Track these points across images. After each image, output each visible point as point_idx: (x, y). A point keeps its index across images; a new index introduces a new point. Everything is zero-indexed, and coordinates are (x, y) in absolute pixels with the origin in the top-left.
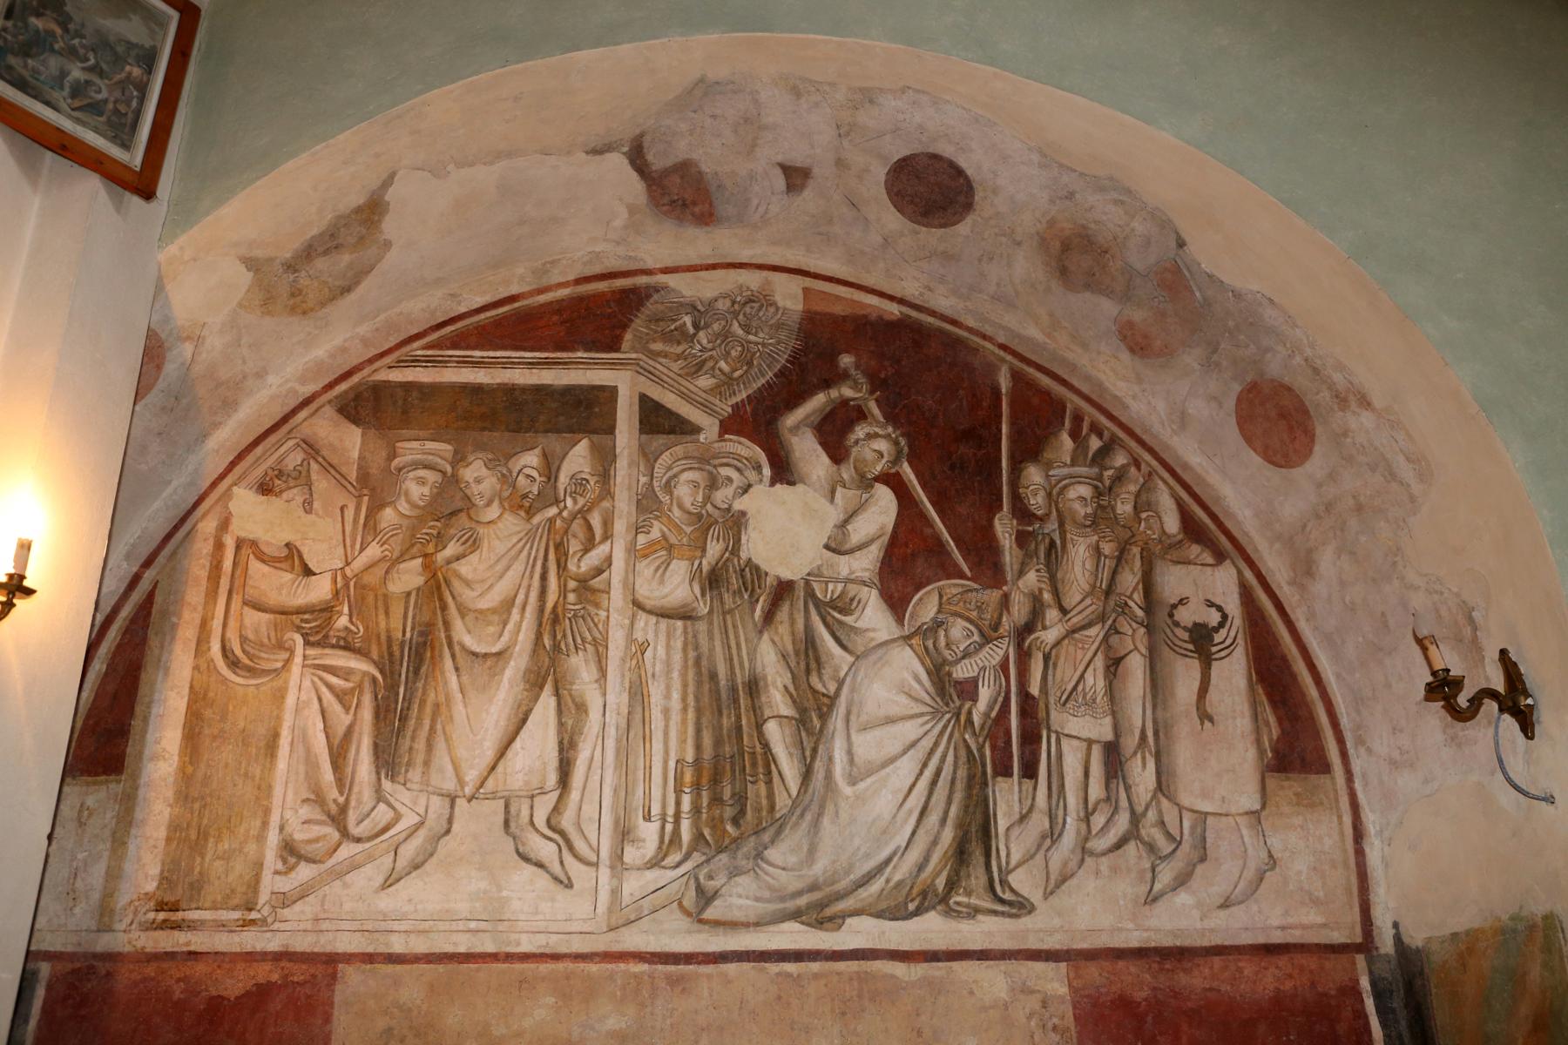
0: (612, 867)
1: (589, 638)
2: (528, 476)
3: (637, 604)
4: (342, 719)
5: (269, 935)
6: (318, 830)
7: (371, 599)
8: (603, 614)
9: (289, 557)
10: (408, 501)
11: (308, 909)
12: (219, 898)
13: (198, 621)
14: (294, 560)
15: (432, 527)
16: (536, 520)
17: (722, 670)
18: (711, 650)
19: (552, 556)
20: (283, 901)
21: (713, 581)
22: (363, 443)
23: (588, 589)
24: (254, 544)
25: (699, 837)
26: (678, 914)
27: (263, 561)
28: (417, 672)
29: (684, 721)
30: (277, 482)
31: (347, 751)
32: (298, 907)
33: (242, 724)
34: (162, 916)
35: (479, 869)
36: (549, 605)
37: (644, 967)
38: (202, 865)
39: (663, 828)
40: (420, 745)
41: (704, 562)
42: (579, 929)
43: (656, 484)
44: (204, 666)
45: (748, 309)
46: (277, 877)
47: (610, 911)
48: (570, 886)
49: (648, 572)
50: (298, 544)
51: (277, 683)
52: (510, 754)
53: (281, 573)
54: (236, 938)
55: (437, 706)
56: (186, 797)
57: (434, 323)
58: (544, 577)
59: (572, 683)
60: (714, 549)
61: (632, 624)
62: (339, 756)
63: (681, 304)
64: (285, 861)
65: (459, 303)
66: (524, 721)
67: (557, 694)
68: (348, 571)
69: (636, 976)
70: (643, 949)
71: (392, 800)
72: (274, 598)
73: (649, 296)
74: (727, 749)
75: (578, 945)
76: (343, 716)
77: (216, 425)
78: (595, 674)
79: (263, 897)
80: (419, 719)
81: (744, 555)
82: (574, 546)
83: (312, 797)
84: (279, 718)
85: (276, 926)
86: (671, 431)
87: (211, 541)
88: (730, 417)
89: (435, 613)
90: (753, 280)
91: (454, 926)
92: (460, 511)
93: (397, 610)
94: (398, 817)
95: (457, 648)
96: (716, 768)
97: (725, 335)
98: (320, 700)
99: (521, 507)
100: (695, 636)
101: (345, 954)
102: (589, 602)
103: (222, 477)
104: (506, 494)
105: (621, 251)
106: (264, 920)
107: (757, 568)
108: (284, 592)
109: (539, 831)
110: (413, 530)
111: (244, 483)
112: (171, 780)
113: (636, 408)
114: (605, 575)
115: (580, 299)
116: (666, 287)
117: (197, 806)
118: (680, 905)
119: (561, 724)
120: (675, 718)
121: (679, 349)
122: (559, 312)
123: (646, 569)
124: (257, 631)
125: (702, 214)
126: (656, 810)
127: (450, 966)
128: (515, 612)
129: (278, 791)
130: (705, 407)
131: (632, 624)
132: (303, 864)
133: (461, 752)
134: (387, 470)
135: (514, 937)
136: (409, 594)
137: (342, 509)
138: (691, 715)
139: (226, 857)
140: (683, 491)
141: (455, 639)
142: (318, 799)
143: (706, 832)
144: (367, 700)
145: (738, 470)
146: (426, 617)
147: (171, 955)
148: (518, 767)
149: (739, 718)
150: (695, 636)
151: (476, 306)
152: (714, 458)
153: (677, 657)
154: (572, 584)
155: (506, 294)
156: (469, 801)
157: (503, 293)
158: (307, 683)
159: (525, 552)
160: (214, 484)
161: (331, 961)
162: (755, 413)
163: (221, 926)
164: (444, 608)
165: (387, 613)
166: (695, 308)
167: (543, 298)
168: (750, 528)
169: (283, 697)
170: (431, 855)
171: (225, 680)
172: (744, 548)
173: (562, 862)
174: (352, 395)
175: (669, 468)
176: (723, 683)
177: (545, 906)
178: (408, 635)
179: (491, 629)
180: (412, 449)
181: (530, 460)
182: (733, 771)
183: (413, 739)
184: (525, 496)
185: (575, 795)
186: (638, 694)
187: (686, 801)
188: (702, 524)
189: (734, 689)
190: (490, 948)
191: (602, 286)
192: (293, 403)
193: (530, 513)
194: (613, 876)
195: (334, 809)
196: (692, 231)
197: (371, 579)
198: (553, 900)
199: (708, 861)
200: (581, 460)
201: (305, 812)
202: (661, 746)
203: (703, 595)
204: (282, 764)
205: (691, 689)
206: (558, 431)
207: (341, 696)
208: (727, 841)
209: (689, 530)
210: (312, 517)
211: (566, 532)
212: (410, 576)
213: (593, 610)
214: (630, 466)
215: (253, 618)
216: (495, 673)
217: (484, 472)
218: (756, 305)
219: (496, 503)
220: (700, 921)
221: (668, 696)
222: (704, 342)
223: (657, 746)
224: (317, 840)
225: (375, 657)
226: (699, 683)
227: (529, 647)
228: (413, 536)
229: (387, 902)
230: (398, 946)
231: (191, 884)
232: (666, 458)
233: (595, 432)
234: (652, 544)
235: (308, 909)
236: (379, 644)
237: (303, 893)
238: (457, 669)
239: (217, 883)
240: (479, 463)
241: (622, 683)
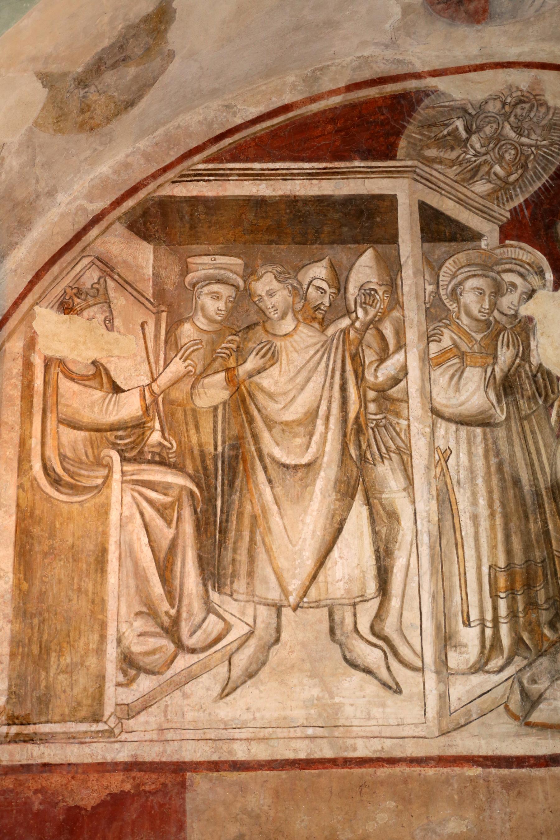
0: (438, 672)
1: (393, 447)
2: (318, 288)
3: (436, 413)
4: (165, 533)
5: (117, 745)
6: (152, 643)
7: (180, 414)
8: (404, 423)
9: (97, 375)
10: (205, 316)
11: (152, 719)
12: (67, 711)
13: (17, 440)
14: (101, 377)
15: (229, 342)
16: (330, 331)
17: (524, 476)
18: (512, 456)
19: (349, 367)
20: (129, 712)
21: (507, 387)
22: (155, 260)
23: (388, 398)
24: (61, 362)
25: (518, 641)
26: (506, 718)
27: (72, 380)
28: (232, 484)
29: (493, 527)
30: (77, 301)
31: (173, 564)
32: (142, 718)
33: (70, 541)
34: (14, 730)
35: (310, 677)
36: (352, 415)
37: (479, 771)
38: (47, 678)
39: (483, 632)
40: (243, 556)
41: (497, 369)
42: (411, 734)
43: (442, 292)
44: (27, 485)
45: (518, 111)
46: (120, 689)
47: (440, 715)
48: (398, 691)
49: (443, 380)
50: (104, 362)
51: (100, 499)
52: (329, 563)
53: (90, 390)
54: (86, 749)
55: (254, 518)
56: (25, 613)
57: (212, 136)
58: (343, 388)
59: (381, 492)
60: (505, 356)
61: (433, 432)
62: (166, 568)
63: (452, 108)
64: (125, 673)
65: (235, 114)
66: (340, 530)
67: (368, 503)
68: (155, 386)
69: (471, 780)
70: (476, 753)
71: (221, 611)
72: (88, 416)
73: (420, 101)
74: (537, 553)
75: (412, 750)
76: (166, 530)
77: (13, 245)
78: (402, 483)
79: (109, 709)
80: (239, 531)
81: (534, 361)
82: (370, 357)
83: (145, 610)
84: (105, 534)
85: (124, 736)
86: (452, 239)
87: (20, 361)
88: (509, 222)
89: (242, 426)
90: (522, 79)
91: (292, 733)
92: (257, 324)
93: (207, 425)
94: (228, 628)
95: (268, 460)
96: (528, 573)
97: (498, 139)
98: (142, 514)
99: (314, 319)
100: (495, 443)
101: (191, 763)
102: (389, 411)
103: (23, 296)
104: (299, 306)
105: (389, 54)
106: (111, 732)
107: (549, 373)
108: (96, 409)
109: (363, 637)
110: (213, 344)
111: (45, 303)
112: (9, 596)
113: (417, 216)
114: (403, 384)
115: (353, 106)
116: (435, 91)
117: (36, 621)
118: (507, 708)
119: (375, 533)
120: (484, 524)
121: (453, 155)
122: (332, 120)
123: (441, 377)
124: (74, 449)
125: (476, 12)
126: (474, 615)
127: (293, 772)
128: (320, 422)
129: (112, 605)
130: (483, 212)
131: (433, 432)
132: (142, 675)
133: (282, 563)
134: (181, 285)
135: (350, 742)
136: (216, 408)
137: (142, 325)
138: (499, 520)
139: (69, 670)
140: (469, 298)
141: (265, 451)
142: (151, 612)
143: (525, 636)
144: (187, 513)
145: (521, 275)
146: (234, 431)
147: (27, 768)
148: (339, 575)
149: (545, 522)
150: (495, 443)
151: (250, 117)
152: (497, 263)
153: (480, 463)
154: (371, 394)
155: (280, 104)
156: (295, 610)
157: (277, 102)
158: (128, 499)
159: (323, 364)
160: (16, 304)
161: (180, 769)
162: (533, 217)
163: (71, 738)
164: (251, 421)
165: (197, 428)
166: (466, 111)
167: (315, 107)
168: (538, 334)
169: (107, 513)
170: (264, 664)
171: (49, 498)
172: (534, 353)
173: (388, 668)
174: (139, 211)
175: (454, 276)
176: (527, 488)
177: (376, 712)
178: (220, 449)
179: (298, 441)
180: (204, 264)
181: (319, 271)
182: (545, 576)
183: (235, 550)
184: (317, 308)
185: (395, 603)
186: (445, 501)
187: (503, 605)
188: (492, 330)
189: (537, 494)
190: (329, 754)
191: (373, 92)
192: (83, 221)
193: (324, 324)
194: (440, 681)
195: (166, 621)
196: (463, 31)
197: (177, 394)
198: (384, 705)
199: (530, 665)
200: (368, 271)
201: (139, 624)
202: (473, 552)
203: (499, 401)
204: (112, 579)
205: (496, 496)
206: (343, 242)
207: (162, 510)
208: (546, 645)
209: (478, 337)
210: (115, 334)
211: (360, 342)
212: (214, 392)
213: (394, 420)
214: (415, 274)
215: (68, 435)
216: (307, 484)
217: (275, 285)
218: (527, 106)
219: (290, 317)
220: (528, 724)
221: (474, 503)
222: (478, 146)
223: (470, 552)
224: (153, 652)
225: (190, 470)
226: (503, 489)
227: (336, 457)
228: (214, 351)
229: (225, 711)
230: (241, 753)
231: (39, 699)
232: (449, 266)
233: (378, 241)
234: (444, 352)
235: (152, 719)
236: (193, 458)
237: (146, 704)
238: (270, 481)
239: (63, 696)
240: (269, 277)
241: (429, 491)
